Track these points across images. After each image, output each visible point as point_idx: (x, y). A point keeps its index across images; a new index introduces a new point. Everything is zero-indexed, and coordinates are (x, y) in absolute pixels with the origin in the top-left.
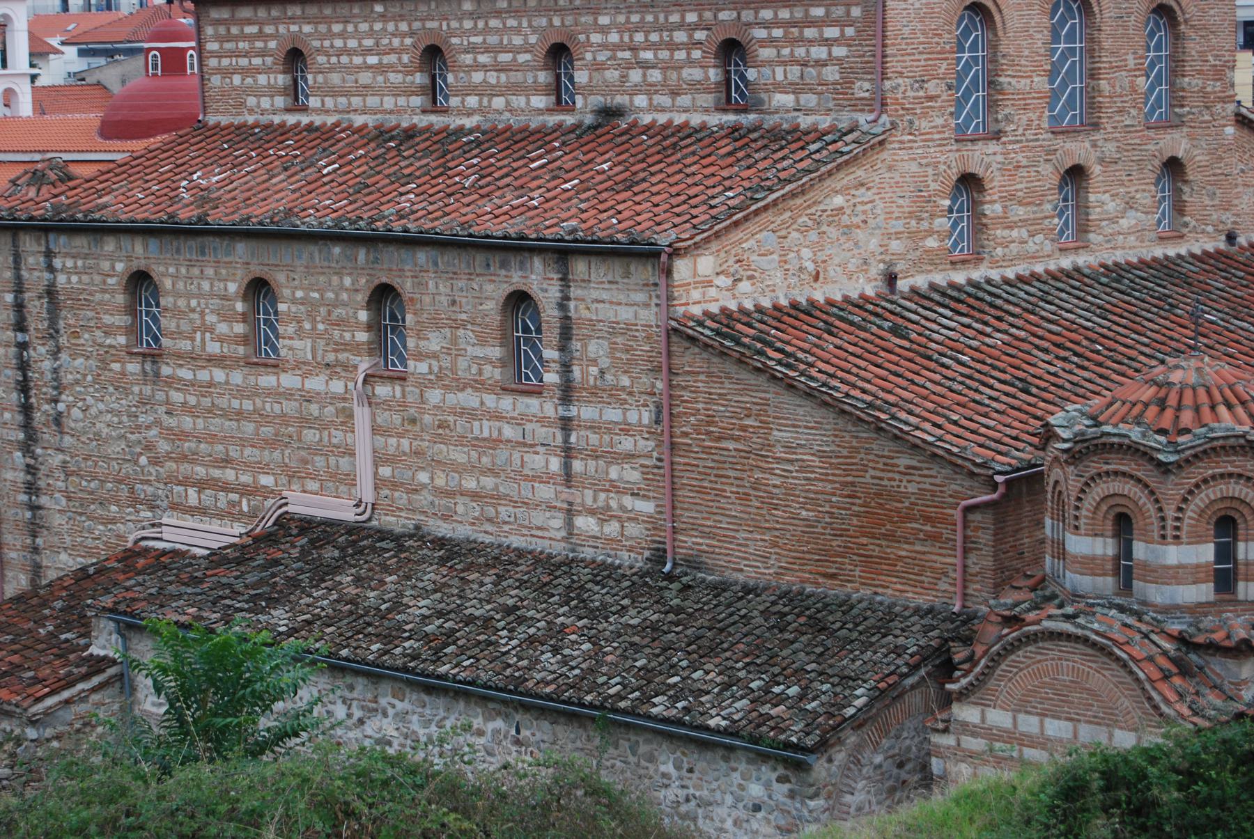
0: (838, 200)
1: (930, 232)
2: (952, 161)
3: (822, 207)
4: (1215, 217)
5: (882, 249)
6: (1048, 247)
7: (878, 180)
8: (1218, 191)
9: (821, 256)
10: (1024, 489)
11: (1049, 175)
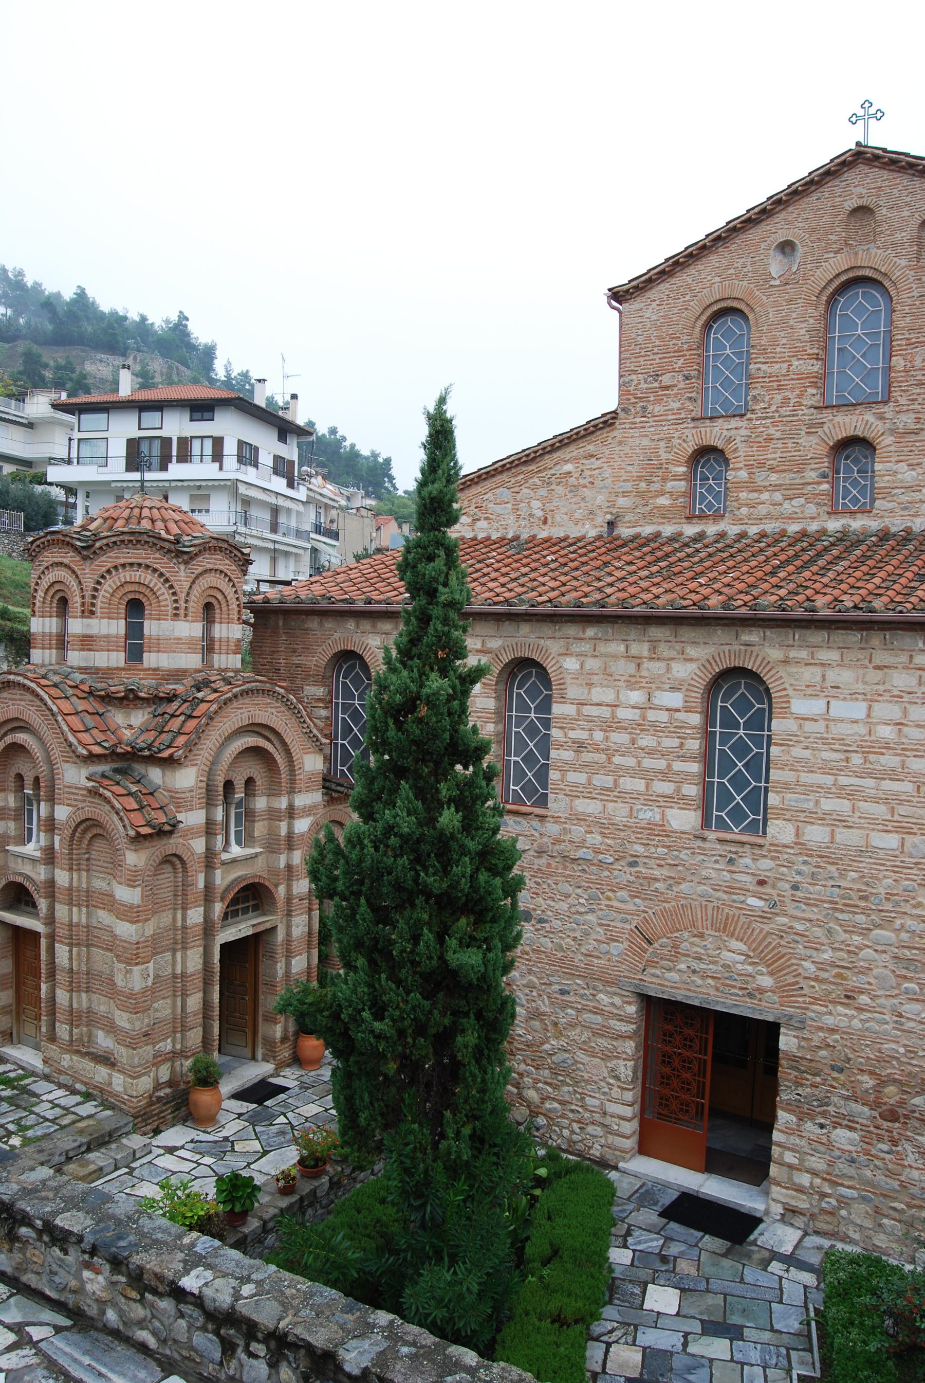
0: (569, 467)
1: (662, 493)
2: (693, 438)
3: (552, 472)
6: (811, 509)
7: (607, 452)
9: (549, 507)
10: (281, 623)
11: (814, 446)
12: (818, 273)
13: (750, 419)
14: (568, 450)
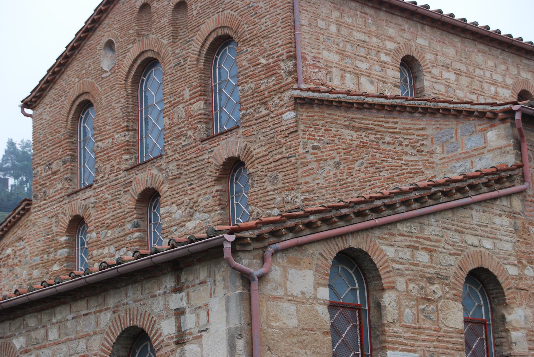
1: (55, 261)
4: (279, 199)
5: (29, 277)
8: (280, 176)
11: (128, 201)
12: (125, 61)
13: (95, 189)
14: (8, 237)
